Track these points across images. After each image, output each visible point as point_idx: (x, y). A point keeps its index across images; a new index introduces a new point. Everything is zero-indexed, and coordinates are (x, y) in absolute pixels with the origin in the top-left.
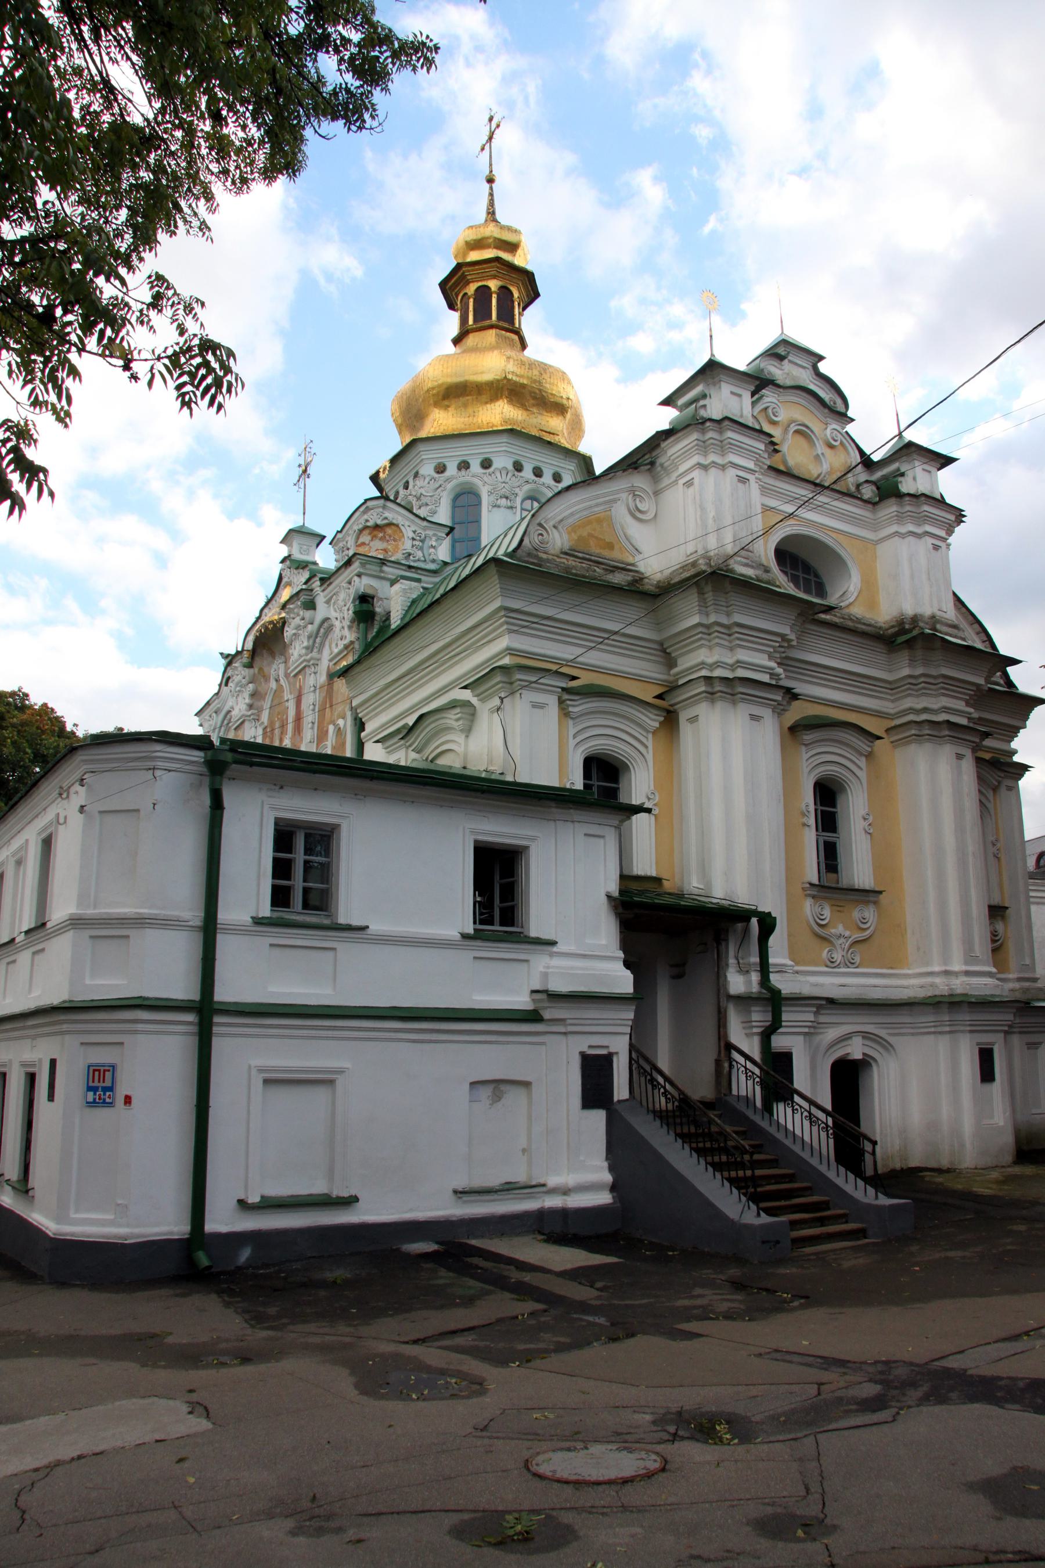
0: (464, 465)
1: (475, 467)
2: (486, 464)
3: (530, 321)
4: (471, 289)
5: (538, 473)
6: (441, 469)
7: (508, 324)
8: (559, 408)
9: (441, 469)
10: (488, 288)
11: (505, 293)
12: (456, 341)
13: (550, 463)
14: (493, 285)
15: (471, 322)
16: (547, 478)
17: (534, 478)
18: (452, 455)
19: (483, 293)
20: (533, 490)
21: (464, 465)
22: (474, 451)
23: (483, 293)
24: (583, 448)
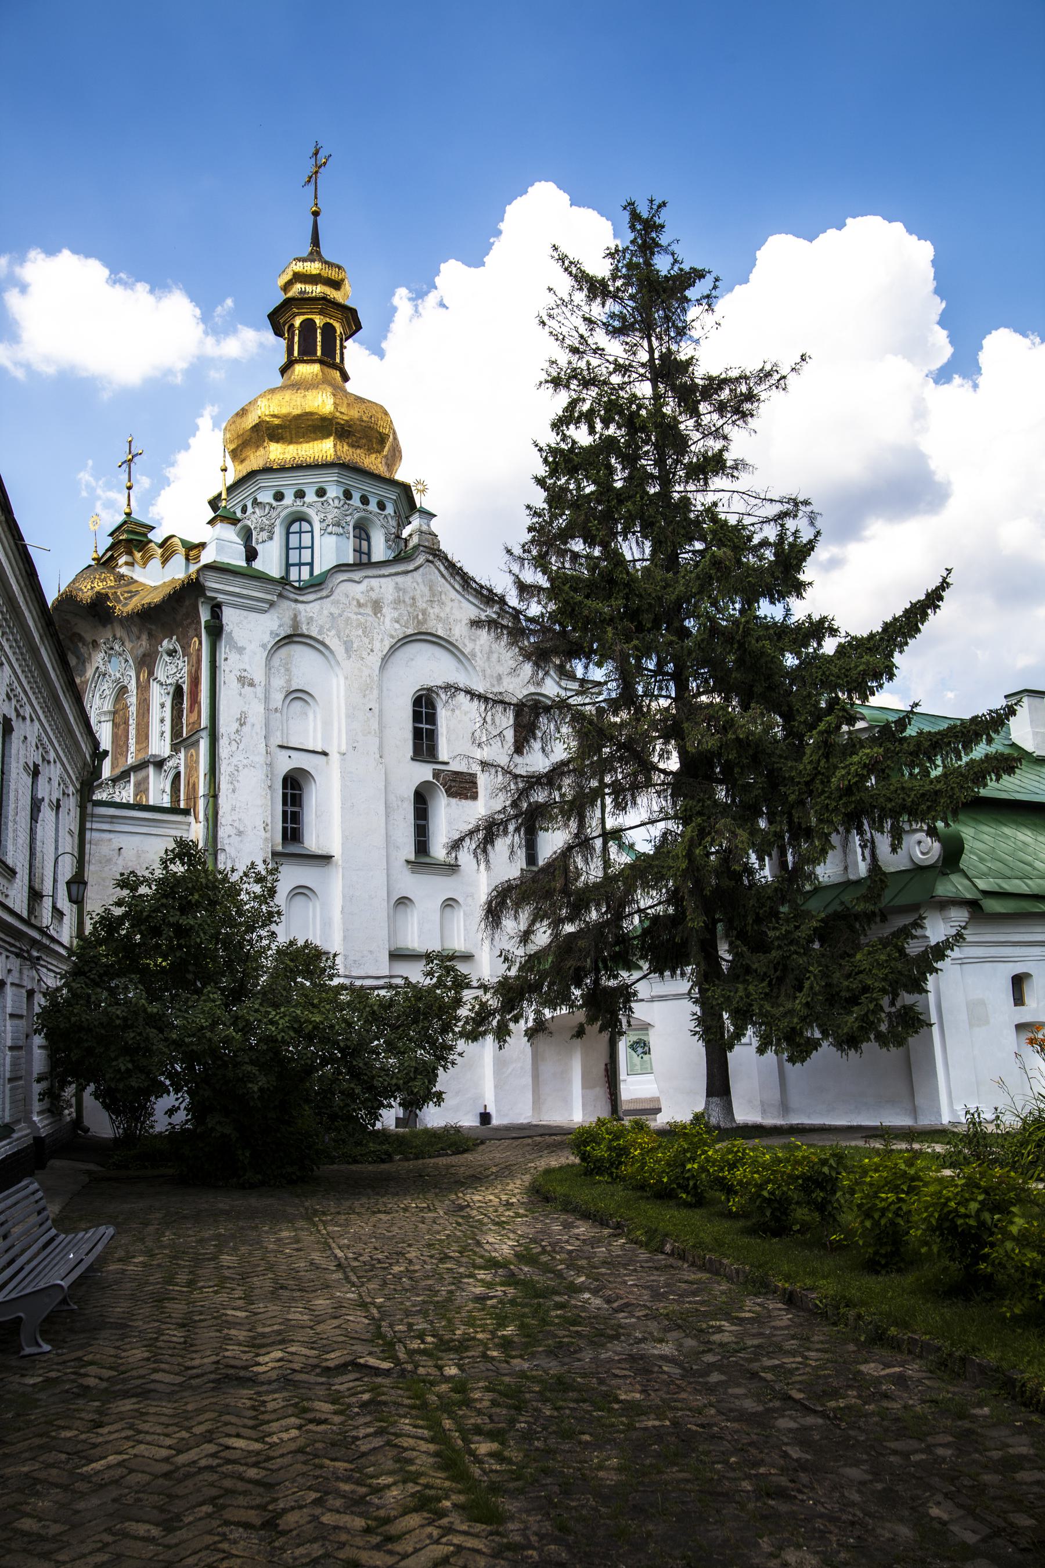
0: (300, 494)
1: (311, 497)
2: (321, 492)
4: (297, 322)
5: (365, 500)
6: (279, 496)
7: (332, 360)
8: (381, 439)
9: (279, 496)
10: (312, 321)
11: (328, 329)
12: (284, 370)
14: (319, 320)
15: (296, 353)
16: (373, 507)
18: (288, 484)
19: (308, 326)
20: (361, 519)
21: (300, 494)
22: (310, 482)
23: (308, 326)
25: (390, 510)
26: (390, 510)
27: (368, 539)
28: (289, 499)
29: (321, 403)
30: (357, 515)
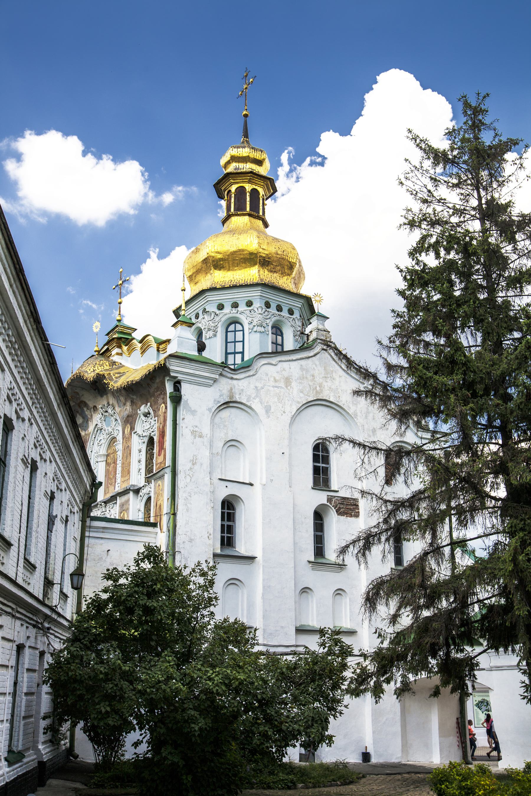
0: (235, 305)
1: (242, 307)
2: (249, 304)
3: (271, 209)
4: (233, 188)
5: (279, 308)
6: (221, 307)
7: (256, 213)
9: (221, 307)
11: (254, 193)
13: (287, 302)
14: (249, 187)
16: (285, 313)
17: (277, 312)
18: (227, 298)
19: (241, 191)
20: (278, 321)
23: (241, 191)
24: (305, 290)
25: (297, 315)
26: (297, 315)
27: (282, 335)
28: (227, 309)
29: (249, 243)
30: (274, 319)
